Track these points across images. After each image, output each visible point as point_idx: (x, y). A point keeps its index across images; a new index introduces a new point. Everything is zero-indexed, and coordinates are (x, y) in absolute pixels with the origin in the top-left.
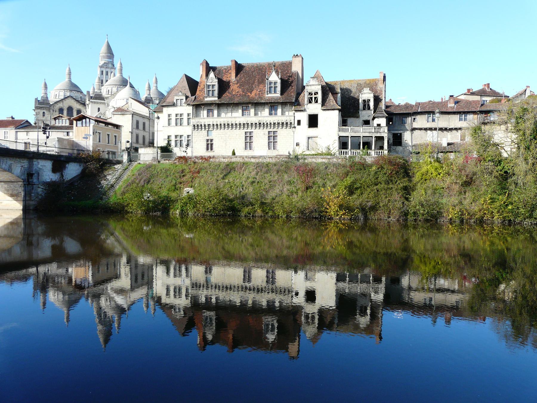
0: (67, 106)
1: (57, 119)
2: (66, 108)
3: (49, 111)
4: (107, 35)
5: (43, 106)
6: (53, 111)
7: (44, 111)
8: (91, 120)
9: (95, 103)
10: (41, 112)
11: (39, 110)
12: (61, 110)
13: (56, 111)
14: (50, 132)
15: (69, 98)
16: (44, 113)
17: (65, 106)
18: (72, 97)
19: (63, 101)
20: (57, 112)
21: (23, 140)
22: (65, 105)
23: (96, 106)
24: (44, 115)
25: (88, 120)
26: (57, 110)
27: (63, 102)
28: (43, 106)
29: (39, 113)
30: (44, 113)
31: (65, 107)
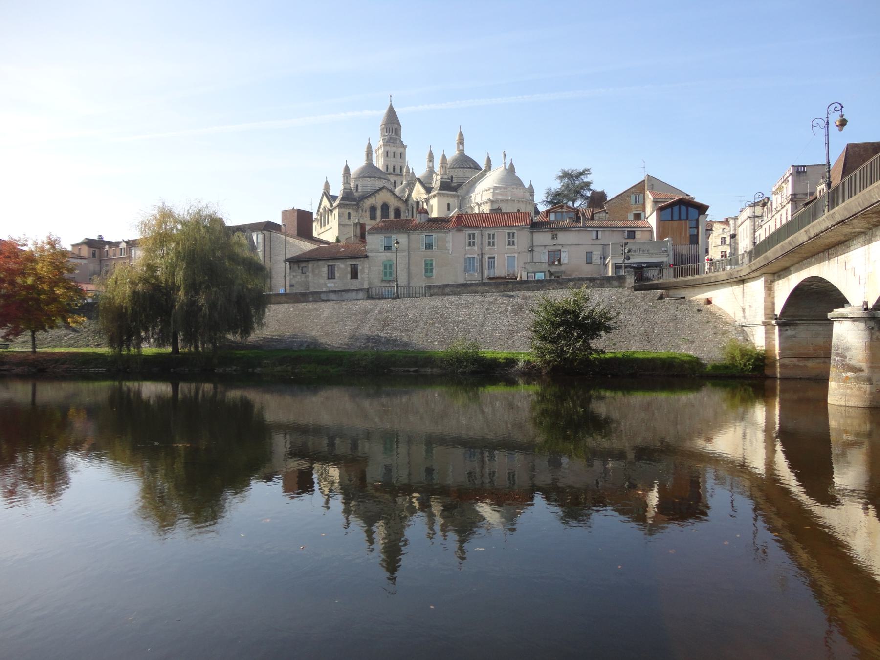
0: (381, 204)
1: (553, 212)
2: (380, 206)
3: (357, 211)
4: (391, 96)
5: (348, 203)
6: (362, 210)
7: (351, 211)
8: (690, 209)
9: (444, 195)
10: (346, 211)
11: (343, 210)
12: (373, 209)
13: (366, 211)
14: (600, 233)
15: (384, 191)
16: (349, 214)
17: (379, 203)
18: (387, 189)
19: (377, 194)
20: (367, 212)
21: (545, 246)
22: (378, 200)
23: (446, 200)
24: (349, 218)
25: (683, 208)
26: (368, 210)
27: (375, 196)
28: (348, 203)
29: (343, 214)
30: (349, 214)
31: (378, 205)
